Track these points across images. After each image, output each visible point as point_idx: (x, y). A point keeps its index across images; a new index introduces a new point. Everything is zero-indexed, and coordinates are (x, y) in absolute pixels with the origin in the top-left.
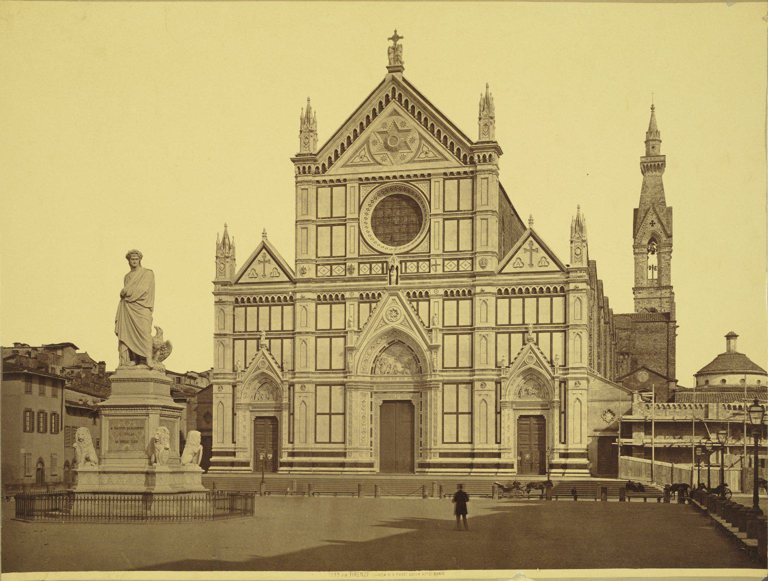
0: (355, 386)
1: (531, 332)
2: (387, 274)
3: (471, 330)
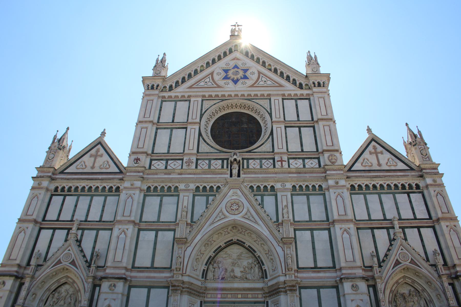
0: (183, 288)
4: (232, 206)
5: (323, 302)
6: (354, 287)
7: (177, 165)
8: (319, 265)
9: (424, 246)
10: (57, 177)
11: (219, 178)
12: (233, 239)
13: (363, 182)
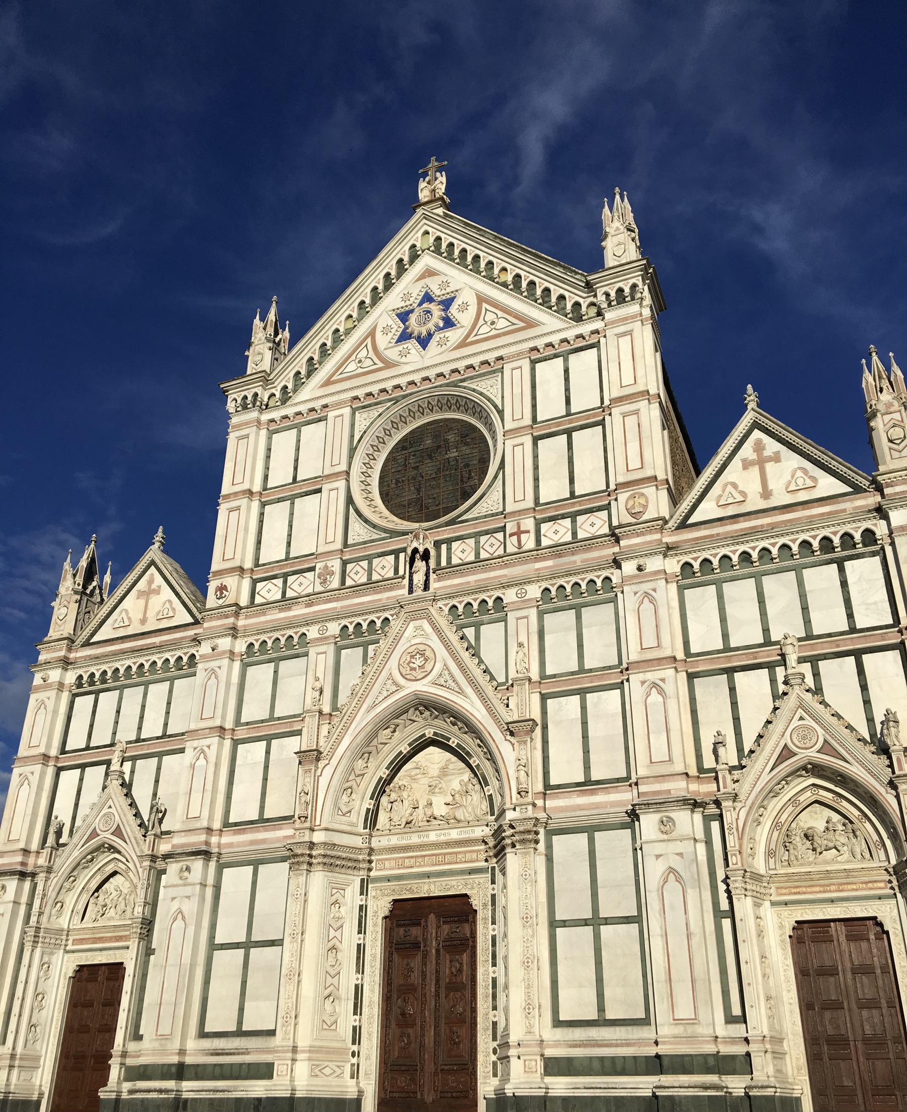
4: (413, 660)
5: (599, 863)
6: (666, 824)
7: (306, 582)
10: (79, 654)
11: (388, 598)
12: (427, 732)
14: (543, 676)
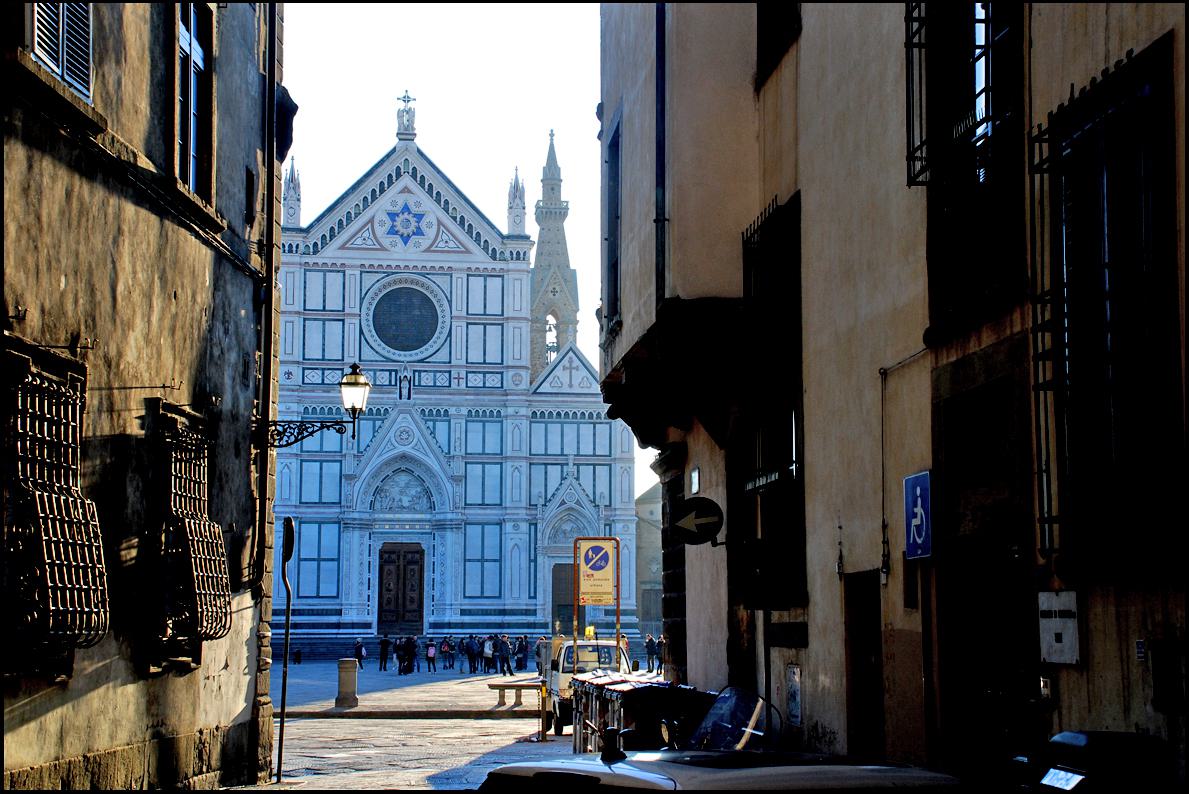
1: (571, 464)
2: (396, 385)
3: (500, 458)
8: (486, 502)
9: (594, 486)
11: (388, 398)
13: (547, 409)
14: (466, 454)
